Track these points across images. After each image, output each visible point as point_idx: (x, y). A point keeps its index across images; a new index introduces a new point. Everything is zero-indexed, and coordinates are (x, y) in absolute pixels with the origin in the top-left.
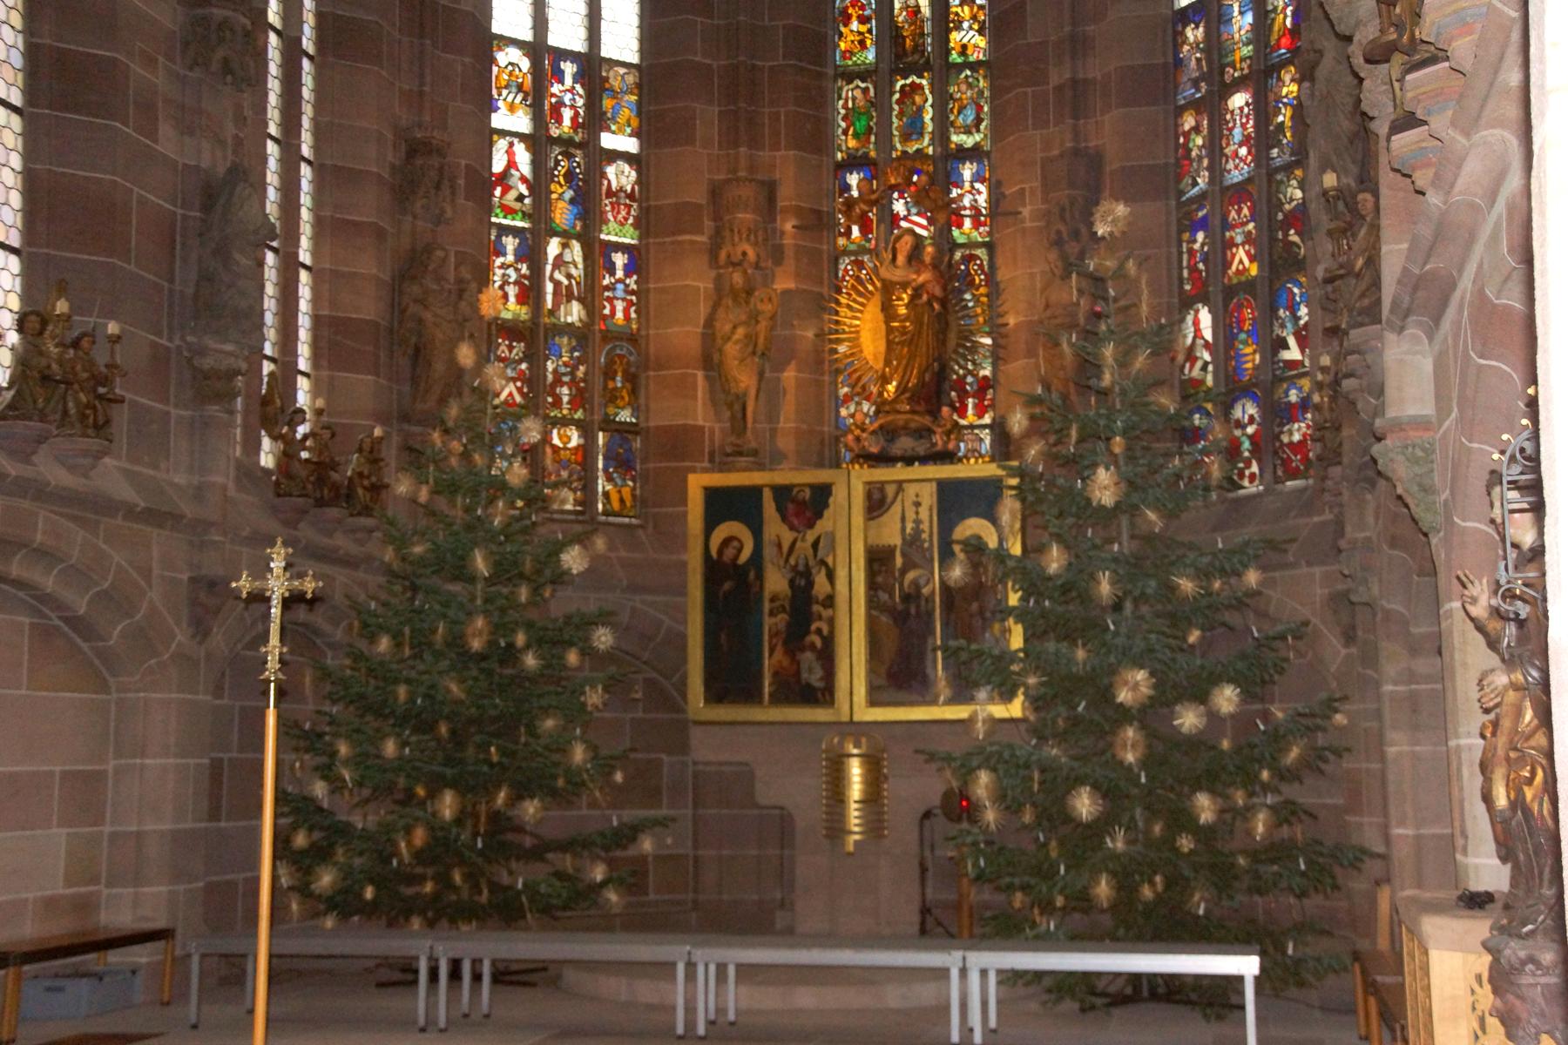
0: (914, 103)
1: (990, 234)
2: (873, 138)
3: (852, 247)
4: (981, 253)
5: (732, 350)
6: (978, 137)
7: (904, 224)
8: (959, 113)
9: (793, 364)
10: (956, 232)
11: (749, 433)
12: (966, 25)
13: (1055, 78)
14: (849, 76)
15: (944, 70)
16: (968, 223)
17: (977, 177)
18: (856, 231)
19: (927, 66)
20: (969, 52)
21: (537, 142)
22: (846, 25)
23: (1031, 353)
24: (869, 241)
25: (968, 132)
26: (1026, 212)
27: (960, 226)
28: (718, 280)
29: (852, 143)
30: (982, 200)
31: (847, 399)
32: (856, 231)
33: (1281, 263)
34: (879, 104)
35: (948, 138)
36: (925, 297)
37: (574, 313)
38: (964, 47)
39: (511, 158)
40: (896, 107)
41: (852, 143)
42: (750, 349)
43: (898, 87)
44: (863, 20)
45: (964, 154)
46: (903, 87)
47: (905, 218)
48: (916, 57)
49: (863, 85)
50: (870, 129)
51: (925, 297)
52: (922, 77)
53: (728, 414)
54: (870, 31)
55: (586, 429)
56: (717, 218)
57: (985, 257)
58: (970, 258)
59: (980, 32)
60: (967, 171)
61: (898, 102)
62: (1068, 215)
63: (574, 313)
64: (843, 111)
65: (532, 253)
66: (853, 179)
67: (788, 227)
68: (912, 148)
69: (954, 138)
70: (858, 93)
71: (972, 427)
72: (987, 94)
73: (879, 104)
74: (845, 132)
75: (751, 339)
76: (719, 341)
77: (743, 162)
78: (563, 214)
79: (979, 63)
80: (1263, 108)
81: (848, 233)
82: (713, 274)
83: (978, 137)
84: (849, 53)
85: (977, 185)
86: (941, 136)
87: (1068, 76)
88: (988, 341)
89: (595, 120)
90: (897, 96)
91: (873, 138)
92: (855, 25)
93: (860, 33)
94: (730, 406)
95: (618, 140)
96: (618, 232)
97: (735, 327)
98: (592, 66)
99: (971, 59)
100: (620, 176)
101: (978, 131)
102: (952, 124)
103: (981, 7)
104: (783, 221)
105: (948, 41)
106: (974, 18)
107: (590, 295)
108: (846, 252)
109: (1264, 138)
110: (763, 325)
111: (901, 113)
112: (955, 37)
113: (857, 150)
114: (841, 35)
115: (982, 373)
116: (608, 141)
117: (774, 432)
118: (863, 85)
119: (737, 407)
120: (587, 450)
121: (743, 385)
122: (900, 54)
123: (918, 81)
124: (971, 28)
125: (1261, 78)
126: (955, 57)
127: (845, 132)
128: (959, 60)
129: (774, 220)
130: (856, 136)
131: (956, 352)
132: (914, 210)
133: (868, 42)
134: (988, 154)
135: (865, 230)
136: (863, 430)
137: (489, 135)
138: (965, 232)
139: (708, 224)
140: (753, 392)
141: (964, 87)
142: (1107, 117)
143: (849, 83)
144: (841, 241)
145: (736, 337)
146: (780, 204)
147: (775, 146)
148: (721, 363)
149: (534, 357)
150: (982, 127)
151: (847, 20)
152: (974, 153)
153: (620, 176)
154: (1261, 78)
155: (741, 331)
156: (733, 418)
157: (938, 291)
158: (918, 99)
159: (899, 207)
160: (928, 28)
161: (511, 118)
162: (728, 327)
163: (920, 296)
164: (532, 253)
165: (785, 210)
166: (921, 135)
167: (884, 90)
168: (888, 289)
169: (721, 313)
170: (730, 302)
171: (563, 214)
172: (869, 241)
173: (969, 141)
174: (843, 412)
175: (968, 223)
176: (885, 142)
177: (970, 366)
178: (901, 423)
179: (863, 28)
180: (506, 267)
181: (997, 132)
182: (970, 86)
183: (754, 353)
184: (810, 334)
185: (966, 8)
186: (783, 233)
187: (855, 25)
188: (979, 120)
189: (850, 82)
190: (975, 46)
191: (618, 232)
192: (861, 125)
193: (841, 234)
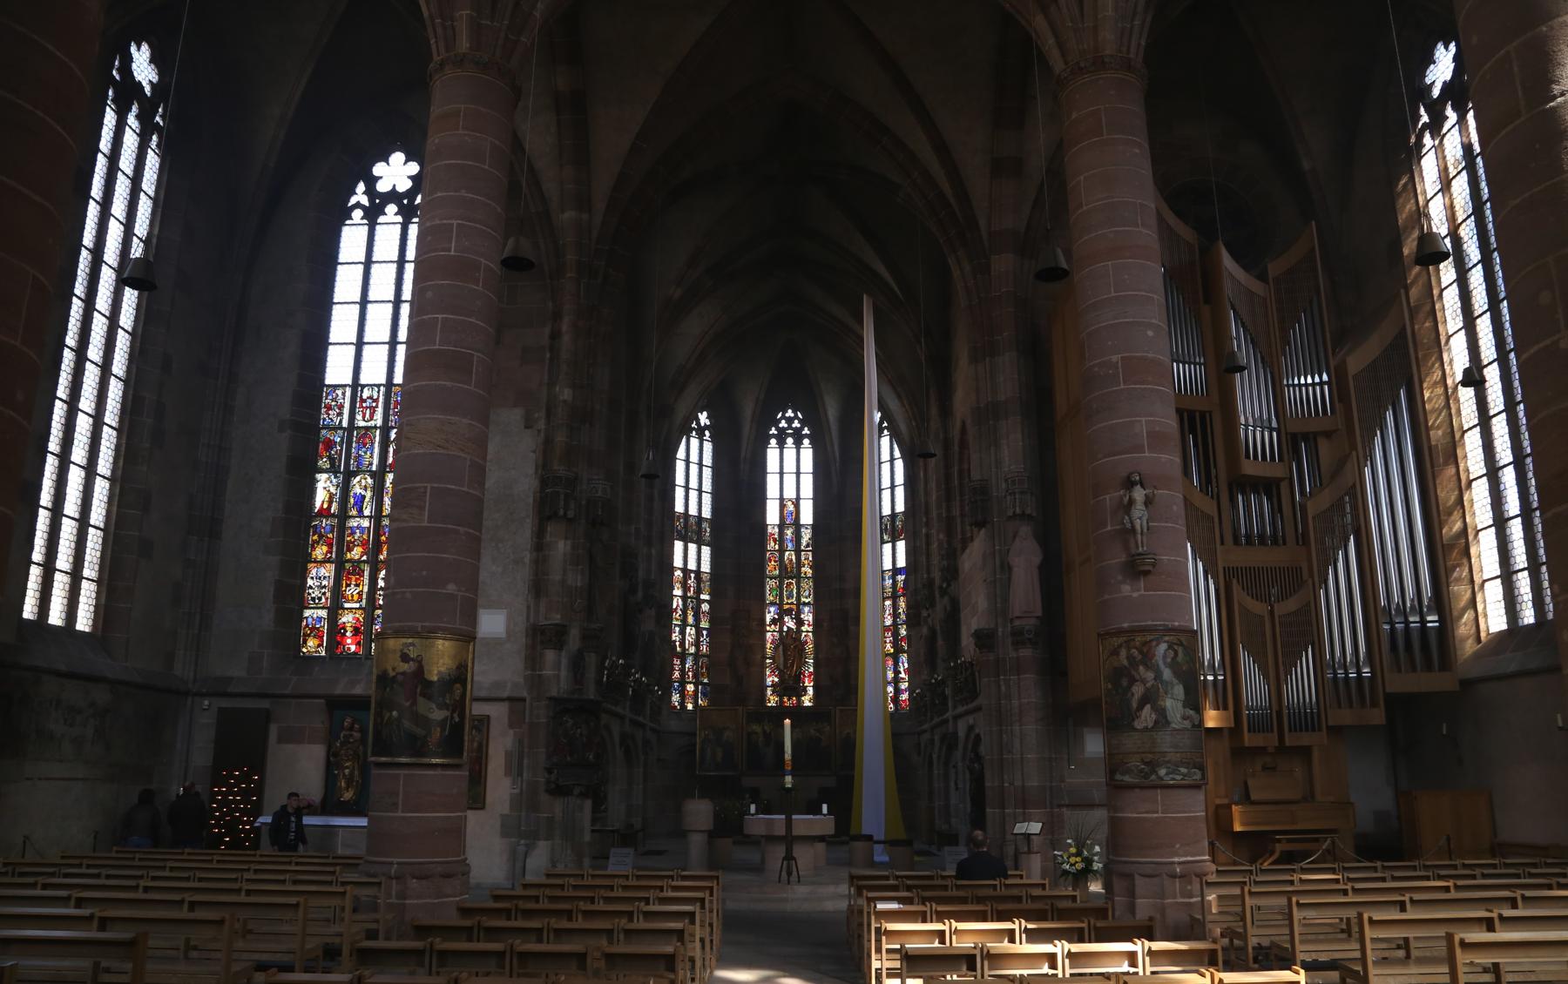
15: (798, 577)
21: (684, 598)
33: (898, 650)
34: (780, 587)
37: (692, 650)
39: (677, 603)
55: (696, 686)
60: (806, 609)
63: (692, 650)
65: (683, 633)
73: (780, 587)
78: (690, 620)
80: (895, 607)
86: (798, 598)
89: (699, 591)
95: (705, 597)
96: (704, 624)
98: (698, 572)
100: (705, 607)
107: (697, 644)
109: (895, 615)
116: (703, 597)
120: (696, 692)
125: (894, 598)
137: (673, 596)
149: (683, 663)
153: (705, 607)
154: (894, 598)
161: (678, 592)
164: (683, 633)
167: (781, 583)
171: (690, 620)
176: (781, 599)
180: (676, 636)
181: (815, 599)
191: (704, 624)
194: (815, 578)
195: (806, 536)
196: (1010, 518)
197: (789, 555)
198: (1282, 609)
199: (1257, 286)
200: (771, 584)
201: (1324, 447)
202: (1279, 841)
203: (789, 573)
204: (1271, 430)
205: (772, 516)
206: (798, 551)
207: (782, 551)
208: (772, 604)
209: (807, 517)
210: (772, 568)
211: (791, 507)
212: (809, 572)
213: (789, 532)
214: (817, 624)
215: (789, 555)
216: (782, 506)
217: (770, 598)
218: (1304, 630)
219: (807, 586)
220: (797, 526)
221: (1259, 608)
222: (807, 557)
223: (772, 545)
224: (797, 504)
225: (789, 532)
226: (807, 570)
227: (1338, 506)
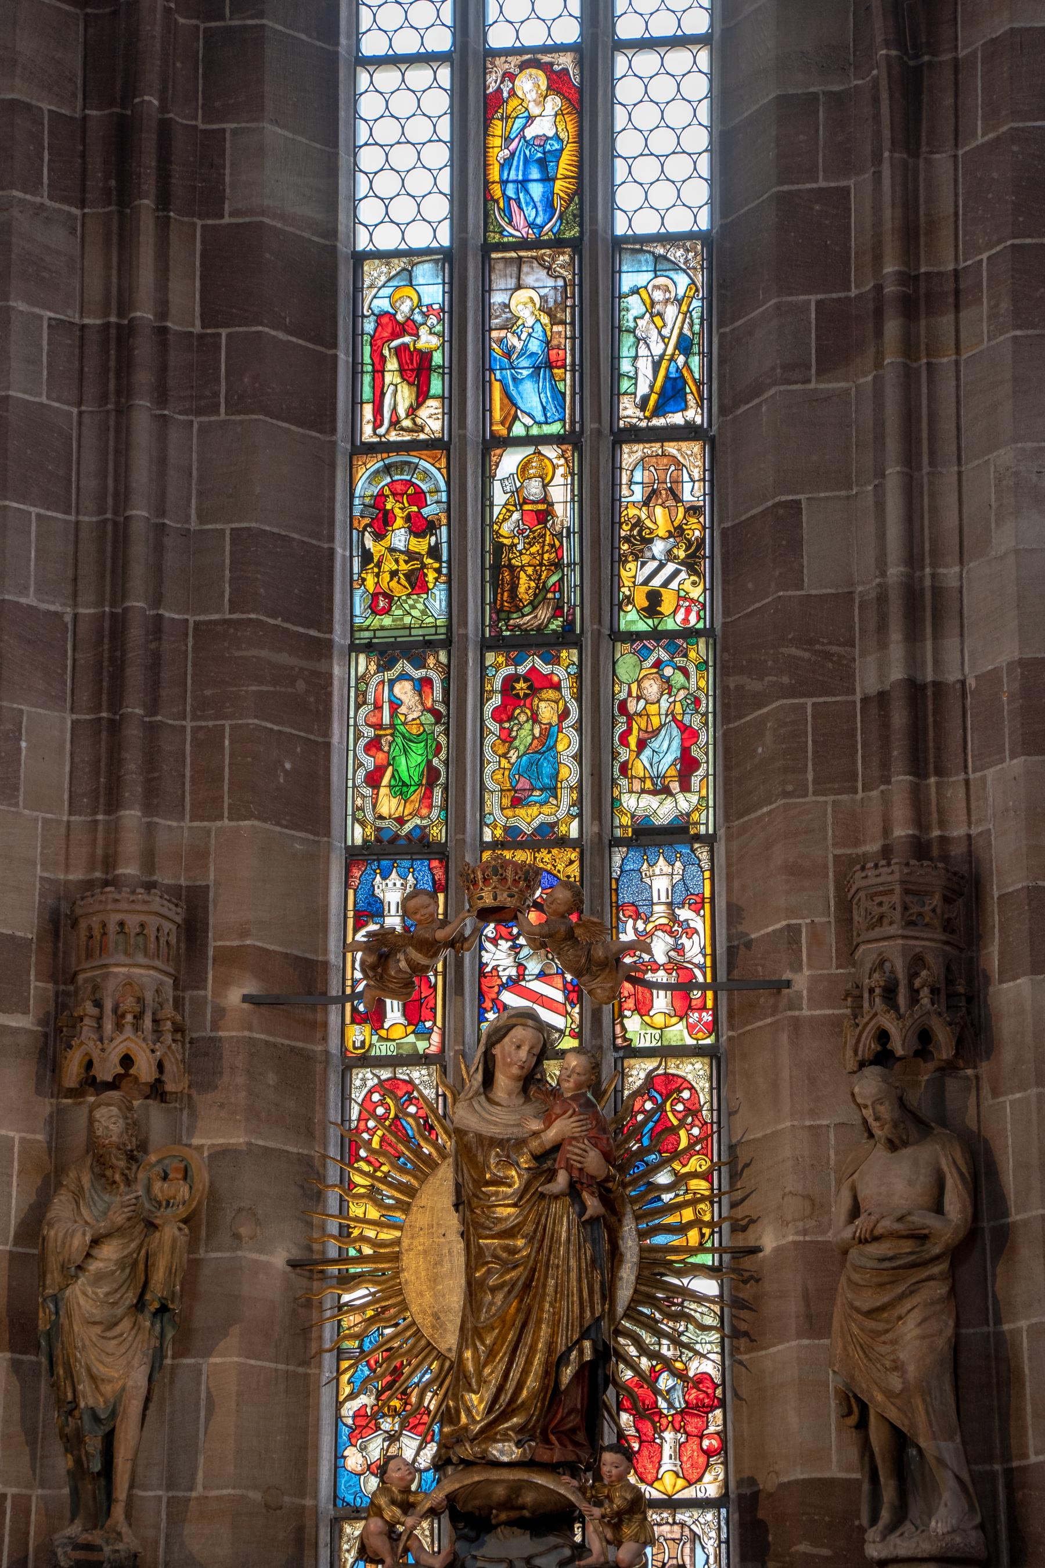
0: (535, 718)
1: (714, 1027)
2: (438, 793)
3: (383, 1049)
4: (695, 1072)
5: (85, 1299)
6: (685, 803)
7: (509, 998)
8: (642, 745)
9: (233, 1339)
10: (633, 1024)
11: (118, 1511)
12: (658, 548)
13: (868, 679)
14: (388, 652)
16: (661, 1001)
17: (684, 896)
18: (394, 1013)
19: (568, 637)
20: (666, 607)
22: (379, 536)
23: (815, 1324)
24: (427, 1034)
25: (666, 791)
26: (801, 981)
27: (643, 1009)
28: (57, 1123)
29: (388, 805)
30: (695, 949)
31: (366, 1423)
32: (394, 1013)
34: (450, 716)
35: (615, 801)
36: (562, 1179)
38: (654, 598)
40: (493, 726)
41: (388, 805)
42: (131, 1298)
43: (498, 684)
44: (420, 527)
45: (649, 837)
46: (509, 682)
47: (514, 984)
48: (543, 614)
49: (418, 674)
50: (432, 774)
51: (562, 1179)
52: (556, 661)
53: (63, 1463)
54: (434, 552)
56: (63, 976)
57: (702, 1085)
58: (667, 1086)
59: (691, 565)
60: (661, 878)
61: (498, 715)
62: (902, 1000)
64: (369, 732)
66: (391, 892)
67: (234, 996)
68: (528, 819)
69: (629, 802)
70: (404, 691)
71: (671, 1504)
72: (707, 704)
74: (373, 780)
75: (139, 1270)
76: (54, 1277)
77: (131, 844)
79: (689, 634)
81: (376, 1018)
82: (46, 1106)
83: (685, 803)
84: (381, 601)
85: (684, 914)
87: (897, 673)
88: (708, 1287)
90: (496, 700)
91: (438, 793)
92: (399, 537)
93: (411, 556)
94: (73, 1442)
97: (96, 1242)
99: (670, 625)
101: (686, 788)
102: (624, 768)
103: (694, 510)
104: (223, 983)
105: (615, 579)
106: (678, 532)
108: (366, 1061)
110: (170, 1232)
111: (508, 739)
112: (632, 573)
113: (401, 821)
114: (367, 557)
115: (696, 1367)
117: (178, 1511)
118: (418, 674)
119: (93, 1444)
121: (107, 1389)
122: (506, 603)
123: (545, 669)
124: (670, 556)
126: (631, 620)
127: (373, 780)
128: (642, 626)
129: (200, 982)
130: (400, 789)
131: (631, 1313)
132: (533, 967)
133: (431, 576)
134: (709, 840)
135: (414, 1014)
136: (407, 1507)
138: (654, 1023)
139: (36, 986)
140: (134, 1407)
141: (652, 688)
142: (990, 773)
143: (383, 668)
144: (357, 1034)
145: (93, 1266)
146: (214, 943)
147: (208, 808)
148: (55, 1331)
150: (695, 781)
151: (382, 524)
152: (675, 835)
155: (109, 1253)
156: (78, 1473)
157: (593, 1161)
158: (547, 712)
159: (498, 957)
160: (570, 552)
162: (78, 1242)
163: (551, 1176)
165: (230, 958)
166: (553, 791)
168: (470, 1151)
169: (61, 1206)
170: (86, 1180)
172: (427, 1034)
173: (662, 811)
174: (354, 1460)
175: (661, 1001)
177: (667, 1350)
178: (500, 1491)
179: (420, 546)
182: (667, 686)
183: (140, 1305)
184: (279, 1259)
185: (659, 510)
186: (220, 1012)
187: (399, 537)
188: (687, 764)
189: (386, 665)
190: (682, 597)
192: (410, 764)
193: (358, 1018)
194: (735, 649)
195: (659, 316)
197: (531, 478)
200: (383, 708)
203: (534, 618)
205: (399, 185)
206: (594, 439)
207: (467, 450)
209: (666, 171)
210: (390, 583)
211: (540, 114)
212: (687, 597)
213: (526, 303)
214: (741, 982)
215: (531, 478)
216: (476, 109)
219: (665, 698)
220: (590, 249)
222: (667, 487)
223: (398, 408)
224: (585, 80)
225: (526, 303)
226: (668, 584)
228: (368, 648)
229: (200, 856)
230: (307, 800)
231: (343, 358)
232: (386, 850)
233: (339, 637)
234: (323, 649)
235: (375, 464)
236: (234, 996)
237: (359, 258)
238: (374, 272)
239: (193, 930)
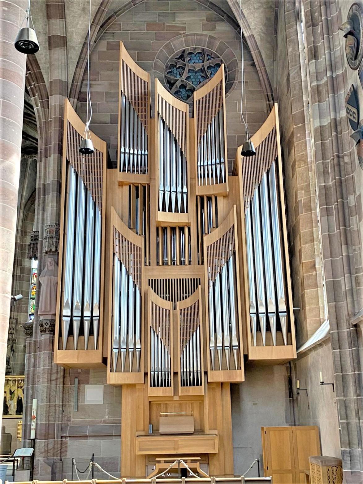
67: (20, 326)
74: (32, 309)
127: (32, 309)
151: (33, 289)
189: (33, 300)
196: (47, 252)
198: (180, 305)
199: (182, 106)
201: (222, 203)
202: (159, 462)
204: (182, 193)
208: (32, 314)
217: (31, 310)
218: (192, 320)
221: (167, 305)
227: (224, 239)
228: (32, 299)
229: (17, 315)
230: (27, 311)
231: (31, 276)
232: (32, 314)
233: (30, 298)
234: (28, 299)
235: (33, 284)
236: (20, 326)
237: (33, 268)
238: (33, 270)
239: (17, 321)
